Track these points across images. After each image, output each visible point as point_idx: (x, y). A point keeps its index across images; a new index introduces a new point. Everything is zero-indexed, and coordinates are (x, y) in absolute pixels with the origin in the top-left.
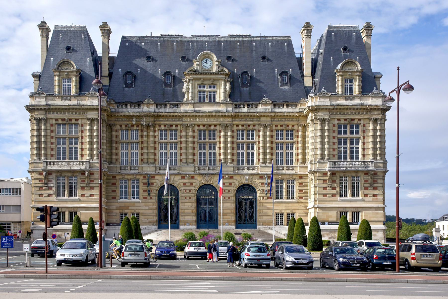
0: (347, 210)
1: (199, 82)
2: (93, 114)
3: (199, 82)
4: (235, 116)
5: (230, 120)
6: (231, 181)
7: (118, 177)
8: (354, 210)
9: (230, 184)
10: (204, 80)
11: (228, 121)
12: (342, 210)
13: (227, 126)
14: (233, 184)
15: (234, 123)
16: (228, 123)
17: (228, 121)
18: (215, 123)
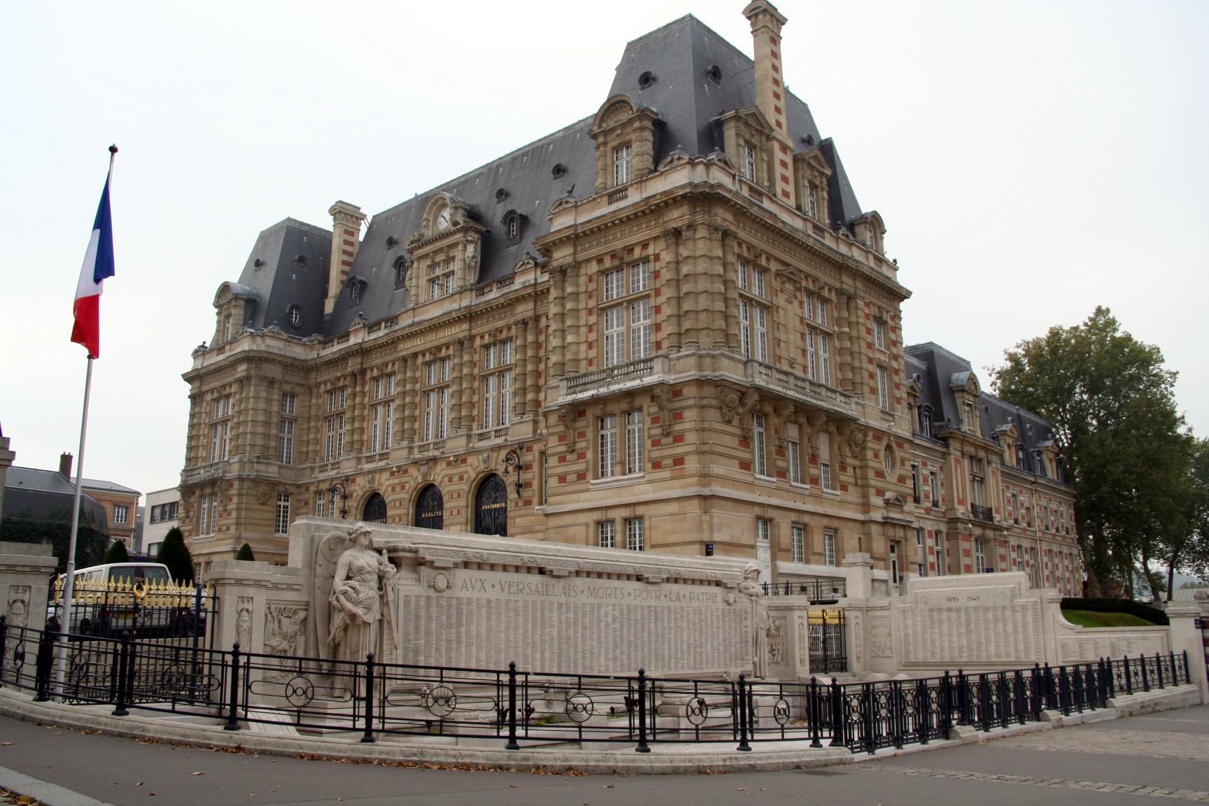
0: (612, 514)
1: (428, 262)
2: (242, 370)
3: (428, 262)
4: (471, 315)
5: (465, 326)
6: (462, 469)
7: (313, 488)
8: (625, 513)
9: (461, 478)
10: (435, 252)
11: (460, 331)
12: (598, 516)
13: (461, 342)
14: (466, 476)
15: (474, 332)
16: (461, 335)
17: (460, 331)
18: (443, 341)
